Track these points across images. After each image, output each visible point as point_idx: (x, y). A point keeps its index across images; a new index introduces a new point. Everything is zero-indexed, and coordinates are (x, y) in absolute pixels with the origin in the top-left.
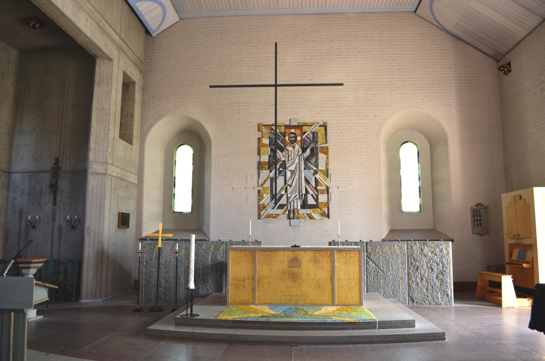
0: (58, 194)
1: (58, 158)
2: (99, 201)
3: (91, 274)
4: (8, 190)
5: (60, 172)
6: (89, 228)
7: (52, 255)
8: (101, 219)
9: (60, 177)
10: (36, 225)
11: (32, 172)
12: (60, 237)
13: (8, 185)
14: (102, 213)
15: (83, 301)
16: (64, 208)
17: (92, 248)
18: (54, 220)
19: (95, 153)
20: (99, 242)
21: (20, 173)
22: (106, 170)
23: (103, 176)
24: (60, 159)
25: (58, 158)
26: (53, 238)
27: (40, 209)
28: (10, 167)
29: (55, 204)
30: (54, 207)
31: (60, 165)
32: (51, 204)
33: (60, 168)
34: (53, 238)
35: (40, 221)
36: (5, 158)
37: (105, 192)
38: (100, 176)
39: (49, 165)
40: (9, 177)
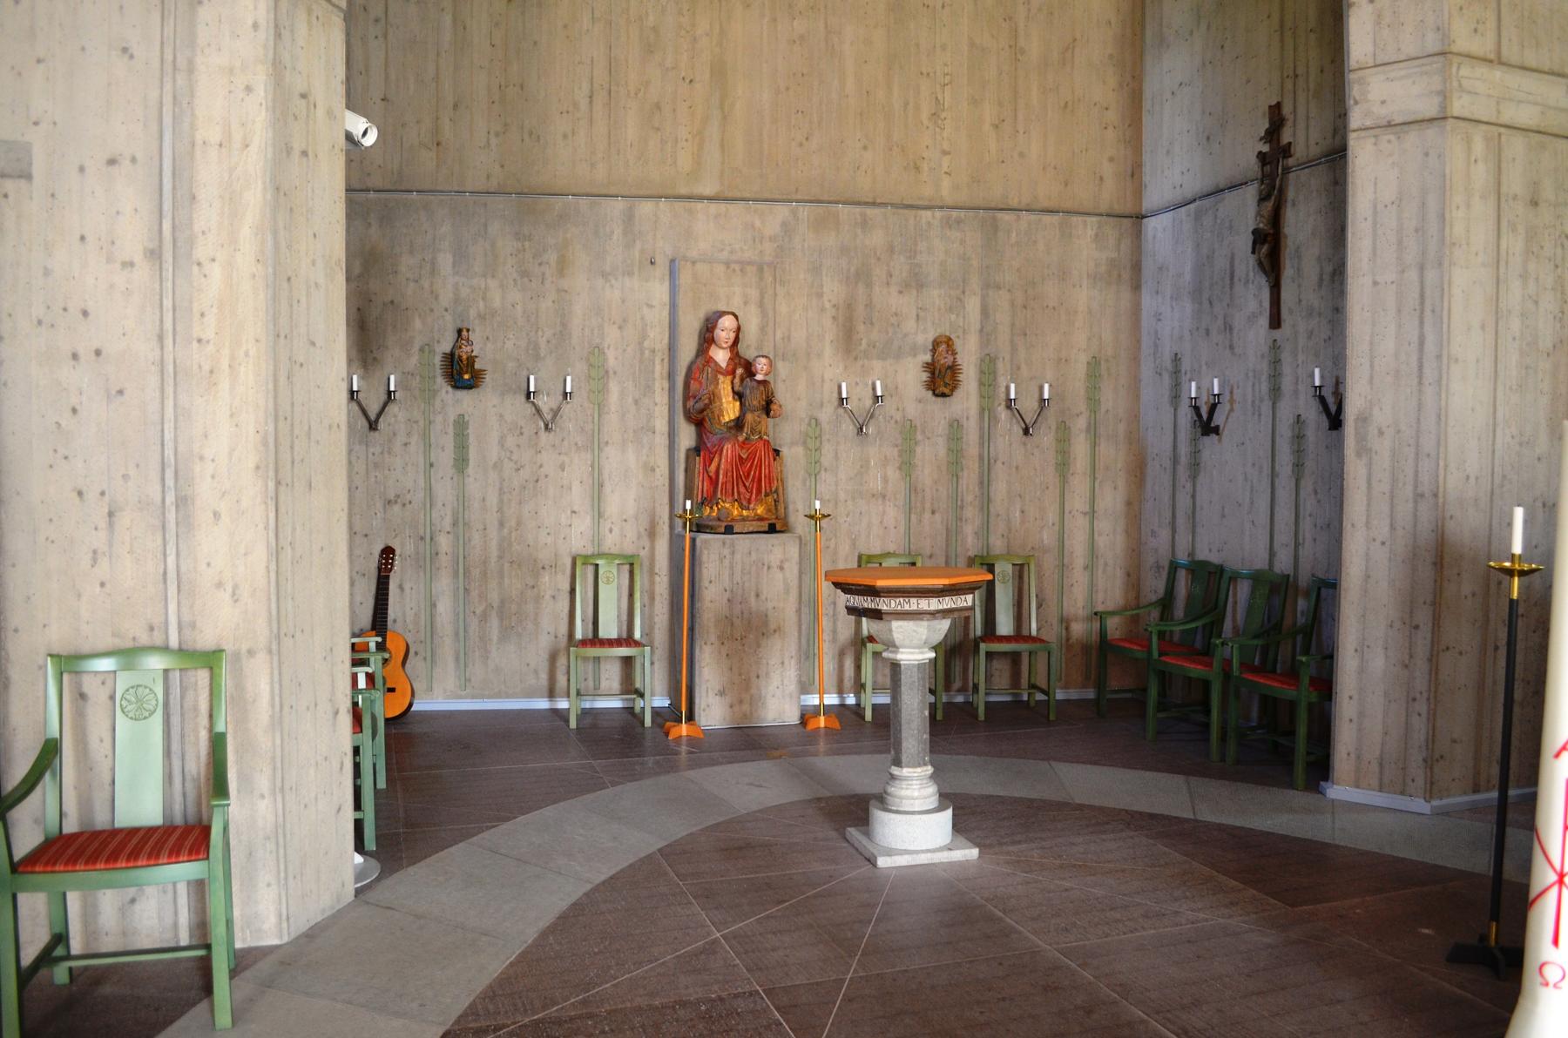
0: (1288, 273)
1: (1278, 105)
2: (1413, 275)
3: (1378, 663)
4: (1136, 287)
5: (1287, 170)
6: (1363, 419)
7: (1272, 554)
8: (1429, 373)
9: (1291, 194)
10: (1218, 419)
11: (1201, 197)
12: (1298, 466)
13: (1137, 267)
14: (1430, 339)
15: (1338, 791)
16: (1310, 334)
17: (1383, 531)
18: (1275, 392)
19: (1379, 17)
20: (1419, 496)
21: (1167, 209)
22: (1444, 95)
23: (1431, 132)
24: (1287, 110)
25: (1278, 105)
26: (1273, 475)
27: (1231, 347)
28: (1139, 191)
29: (1276, 322)
30: (1277, 334)
31: (1286, 137)
32: (1264, 321)
33: (1286, 151)
34: (1273, 475)
35: (1232, 401)
36: (1111, 159)
37: (1442, 217)
38: (1412, 137)
39: (1245, 152)
40: (1138, 234)
